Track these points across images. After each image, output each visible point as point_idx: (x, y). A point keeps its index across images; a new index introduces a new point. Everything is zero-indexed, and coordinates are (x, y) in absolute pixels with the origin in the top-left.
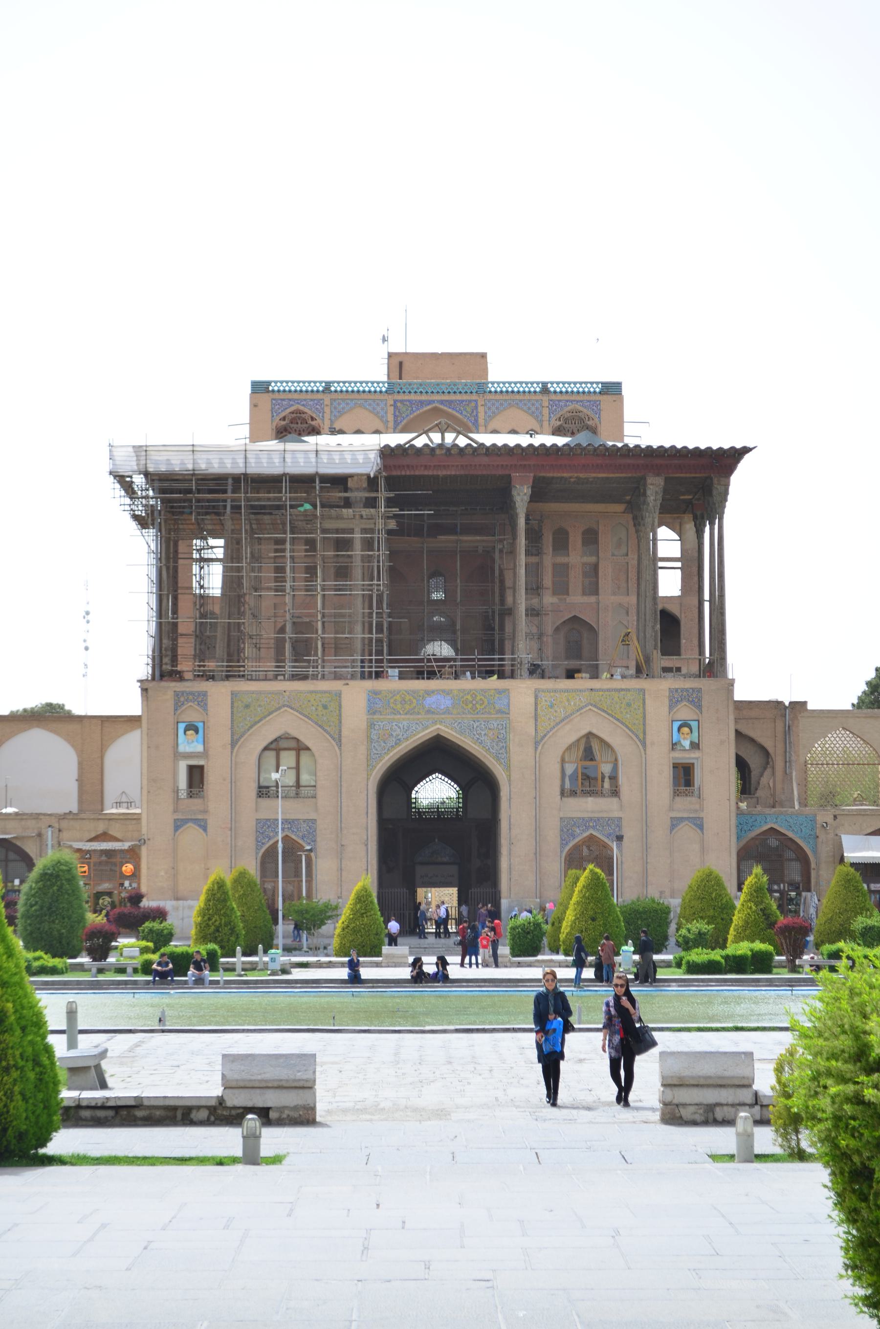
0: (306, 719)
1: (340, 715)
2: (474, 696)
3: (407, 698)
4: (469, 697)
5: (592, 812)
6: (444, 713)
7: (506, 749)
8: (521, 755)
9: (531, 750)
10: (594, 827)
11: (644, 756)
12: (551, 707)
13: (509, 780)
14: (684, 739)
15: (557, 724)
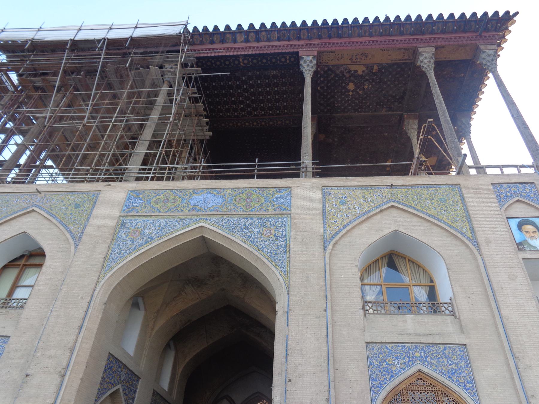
0: (51, 218)
1: (90, 214)
2: (249, 195)
3: (171, 197)
4: (244, 196)
5: (416, 334)
6: (212, 210)
7: (286, 249)
8: (305, 254)
9: (318, 248)
10: (423, 360)
11: (479, 257)
12: (344, 203)
13: (288, 287)
14: (531, 238)
15: (352, 221)
